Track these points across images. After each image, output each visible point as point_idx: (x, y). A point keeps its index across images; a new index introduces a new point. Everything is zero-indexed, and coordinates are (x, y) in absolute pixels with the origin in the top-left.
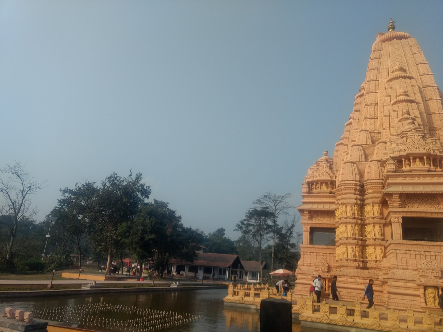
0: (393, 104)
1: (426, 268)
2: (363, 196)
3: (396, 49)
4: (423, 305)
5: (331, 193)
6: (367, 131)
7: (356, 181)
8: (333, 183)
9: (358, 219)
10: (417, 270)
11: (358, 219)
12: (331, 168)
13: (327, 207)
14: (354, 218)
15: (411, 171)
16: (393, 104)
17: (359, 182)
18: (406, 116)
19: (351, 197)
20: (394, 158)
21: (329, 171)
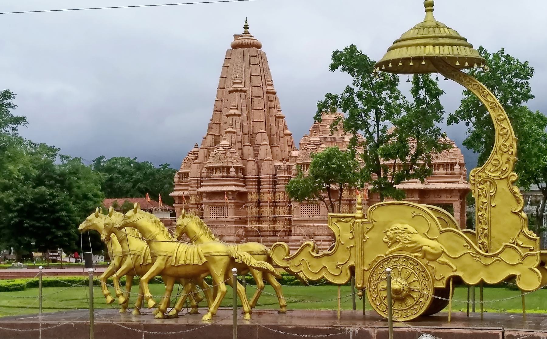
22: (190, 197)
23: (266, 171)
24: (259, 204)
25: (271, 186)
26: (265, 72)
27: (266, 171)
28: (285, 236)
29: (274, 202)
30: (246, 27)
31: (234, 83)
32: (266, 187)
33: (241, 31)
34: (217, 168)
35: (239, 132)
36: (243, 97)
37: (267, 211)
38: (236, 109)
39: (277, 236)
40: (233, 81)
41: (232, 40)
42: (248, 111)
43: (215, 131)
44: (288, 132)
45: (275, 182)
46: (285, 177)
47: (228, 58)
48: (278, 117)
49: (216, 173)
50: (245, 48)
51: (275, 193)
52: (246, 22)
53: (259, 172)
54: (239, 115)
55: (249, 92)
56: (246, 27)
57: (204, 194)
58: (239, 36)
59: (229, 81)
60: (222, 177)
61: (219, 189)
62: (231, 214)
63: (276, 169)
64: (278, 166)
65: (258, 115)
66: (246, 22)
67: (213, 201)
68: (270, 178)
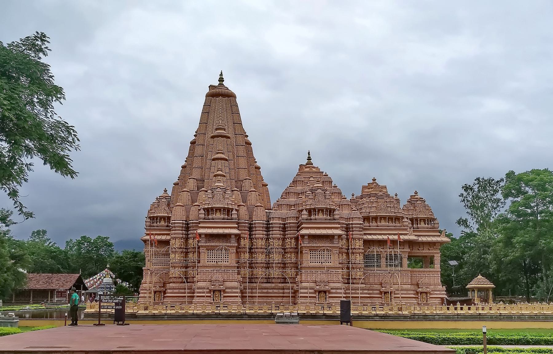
0: (214, 160)
2: (188, 231)
4: (212, 301)
5: (167, 226)
8: (169, 218)
9: (183, 248)
11: (183, 248)
12: (168, 205)
13: (164, 238)
14: (181, 248)
15: (213, 219)
16: (214, 160)
17: (186, 221)
19: (179, 233)
20: (204, 209)
21: (167, 209)
23: (259, 217)
25: (265, 233)
26: (238, 123)
27: (259, 217)
28: (280, 283)
30: (221, 80)
31: (216, 129)
32: (259, 233)
33: (216, 83)
35: (228, 175)
37: (260, 258)
40: (215, 127)
41: (207, 90)
43: (196, 174)
45: (268, 228)
46: (280, 224)
47: (207, 106)
49: (216, 214)
50: (220, 97)
51: (267, 239)
52: (221, 75)
53: (251, 218)
54: (226, 160)
59: (210, 128)
60: (223, 219)
61: (221, 231)
62: (232, 260)
63: (268, 216)
65: (243, 163)
66: (221, 75)
68: (263, 224)
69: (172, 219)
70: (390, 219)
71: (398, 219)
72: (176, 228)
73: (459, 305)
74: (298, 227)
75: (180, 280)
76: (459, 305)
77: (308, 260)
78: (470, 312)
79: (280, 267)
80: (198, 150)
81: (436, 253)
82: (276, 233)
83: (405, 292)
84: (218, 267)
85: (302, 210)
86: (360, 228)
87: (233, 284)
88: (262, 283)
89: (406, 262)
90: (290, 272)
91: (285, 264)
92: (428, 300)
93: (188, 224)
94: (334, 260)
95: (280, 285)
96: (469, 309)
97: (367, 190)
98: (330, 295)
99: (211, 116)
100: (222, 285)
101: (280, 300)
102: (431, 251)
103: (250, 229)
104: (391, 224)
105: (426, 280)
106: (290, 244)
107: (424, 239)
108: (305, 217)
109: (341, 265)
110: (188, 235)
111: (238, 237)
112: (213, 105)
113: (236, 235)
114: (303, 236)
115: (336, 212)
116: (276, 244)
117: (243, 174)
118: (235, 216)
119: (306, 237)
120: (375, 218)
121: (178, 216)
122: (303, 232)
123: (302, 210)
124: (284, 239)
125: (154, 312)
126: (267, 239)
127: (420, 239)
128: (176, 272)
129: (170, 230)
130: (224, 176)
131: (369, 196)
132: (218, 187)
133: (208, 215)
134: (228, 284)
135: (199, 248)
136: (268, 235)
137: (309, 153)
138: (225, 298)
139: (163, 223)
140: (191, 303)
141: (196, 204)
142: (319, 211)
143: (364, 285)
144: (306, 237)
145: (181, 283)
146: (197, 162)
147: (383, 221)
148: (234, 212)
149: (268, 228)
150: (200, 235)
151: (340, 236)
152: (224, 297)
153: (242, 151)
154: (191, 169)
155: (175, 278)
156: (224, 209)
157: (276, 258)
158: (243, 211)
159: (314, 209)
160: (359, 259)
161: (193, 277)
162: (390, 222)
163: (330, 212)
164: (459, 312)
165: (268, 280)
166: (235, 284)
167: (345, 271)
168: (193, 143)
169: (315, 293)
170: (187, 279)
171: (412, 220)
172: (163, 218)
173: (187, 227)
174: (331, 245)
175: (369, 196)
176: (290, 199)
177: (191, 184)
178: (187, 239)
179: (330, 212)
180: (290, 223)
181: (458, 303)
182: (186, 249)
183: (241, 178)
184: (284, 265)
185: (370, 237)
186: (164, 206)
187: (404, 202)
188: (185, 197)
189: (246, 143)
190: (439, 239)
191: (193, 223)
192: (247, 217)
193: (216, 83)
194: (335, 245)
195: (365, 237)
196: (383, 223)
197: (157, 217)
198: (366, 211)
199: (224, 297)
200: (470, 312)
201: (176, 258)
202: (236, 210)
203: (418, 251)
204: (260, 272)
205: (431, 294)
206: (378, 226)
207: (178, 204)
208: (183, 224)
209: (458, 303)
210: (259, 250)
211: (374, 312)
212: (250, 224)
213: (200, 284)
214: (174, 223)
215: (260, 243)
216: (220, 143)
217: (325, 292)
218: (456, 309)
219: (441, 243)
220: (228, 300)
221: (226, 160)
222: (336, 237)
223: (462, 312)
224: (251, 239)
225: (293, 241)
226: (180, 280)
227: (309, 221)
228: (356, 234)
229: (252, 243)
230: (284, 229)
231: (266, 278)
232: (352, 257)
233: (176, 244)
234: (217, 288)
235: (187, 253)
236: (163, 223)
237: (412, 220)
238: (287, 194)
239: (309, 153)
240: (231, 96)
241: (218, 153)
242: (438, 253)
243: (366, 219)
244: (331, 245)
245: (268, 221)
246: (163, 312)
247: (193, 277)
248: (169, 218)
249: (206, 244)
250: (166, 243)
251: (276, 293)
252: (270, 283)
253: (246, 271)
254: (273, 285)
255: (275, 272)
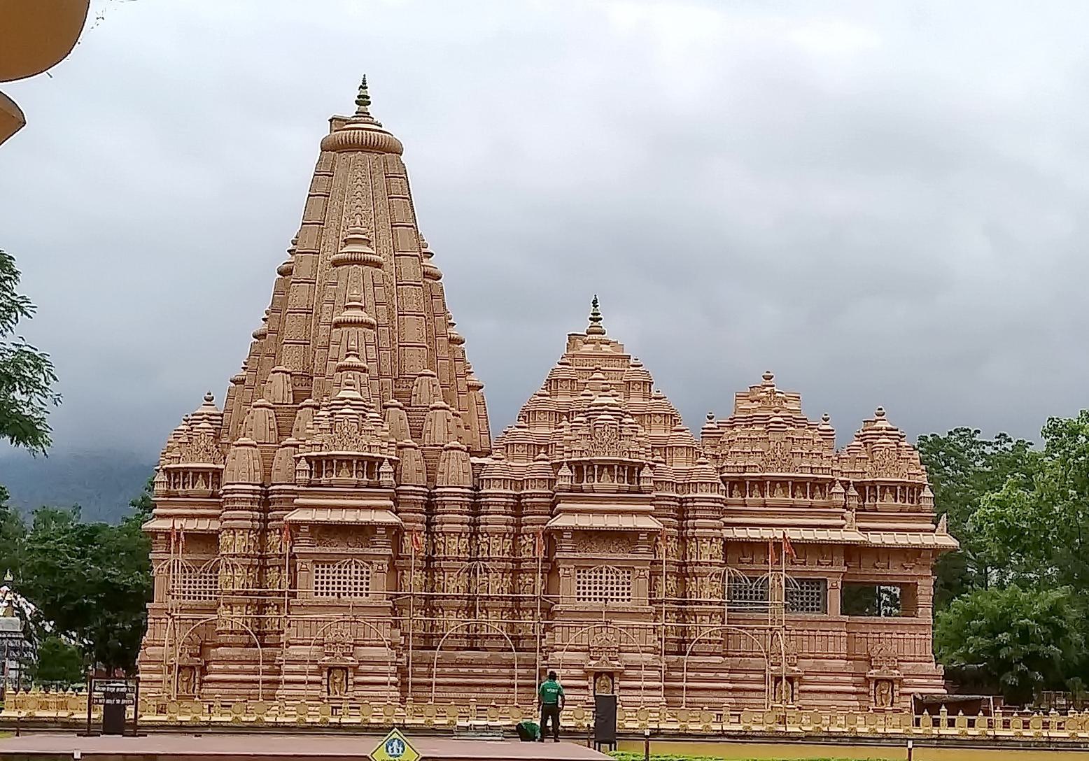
0: (337, 325)
1: (334, 641)
3: (359, 181)
4: (325, 695)
6: (286, 373)
7: (253, 485)
8: (218, 473)
10: (322, 645)
11: (254, 556)
12: (217, 437)
13: (203, 525)
16: (337, 325)
17: (262, 485)
18: (353, 360)
19: (243, 517)
22: (225, 538)
23: (454, 475)
24: (430, 565)
27: (454, 475)
29: (429, 560)
30: (363, 101)
32: (453, 520)
33: (350, 110)
34: (347, 461)
35: (373, 367)
36: (378, 281)
37: (453, 584)
38: (362, 308)
39: (435, 648)
42: (390, 313)
43: (291, 360)
44: (474, 379)
45: (476, 506)
47: (323, 173)
48: (452, 341)
50: (359, 148)
51: (474, 535)
52: (363, 87)
54: (371, 326)
55: (389, 268)
56: (363, 101)
57: (305, 529)
58: (347, 121)
59: (330, 237)
61: (350, 517)
62: (377, 591)
63: (476, 475)
64: (483, 465)
65: (414, 331)
66: (363, 87)
67: (328, 550)
69: (227, 477)
70: (798, 485)
71: (819, 485)
72: (236, 505)
73: (944, 716)
74: (553, 505)
75: (245, 639)
76: (944, 716)
77: (569, 591)
78: (971, 732)
79: (504, 609)
80: (300, 296)
81: (921, 577)
82: (496, 520)
83: (831, 678)
84: (341, 607)
85: (560, 465)
86: (714, 509)
87: (378, 649)
88: (458, 649)
89: (834, 599)
90: (529, 622)
91: (517, 600)
92: (896, 700)
93: (267, 494)
94: (636, 594)
95: (505, 655)
96: (971, 724)
97: (747, 405)
98: (622, 683)
99: (334, 204)
100: (351, 655)
101: (501, 694)
102: (907, 572)
103: (430, 507)
104: (799, 499)
105: (893, 649)
106: (533, 550)
107: (889, 540)
108: (564, 483)
109: (653, 608)
110: (266, 521)
111: (395, 533)
112: (339, 172)
113: (389, 527)
114: (560, 531)
115: (646, 472)
116: (497, 547)
117: (415, 362)
118: (387, 479)
119: (567, 536)
120: (760, 484)
121: (241, 471)
122: (562, 521)
123: (560, 465)
124: (517, 536)
125: (180, 718)
126: (474, 535)
127: (875, 539)
128: (233, 618)
129: (220, 506)
130: (365, 370)
131: (750, 421)
132: (345, 402)
133: (319, 474)
134: (366, 652)
135: (293, 557)
136: (475, 524)
137: (595, 303)
138: (357, 688)
139: (201, 487)
140: (272, 697)
141: (290, 440)
142: (601, 467)
143: (719, 659)
144: (567, 536)
145: (247, 646)
146: (294, 327)
147: (779, 491)
148: (386, 467)
149: (476, 506)
150: (296, 526)
151: (652, 533)
152: (356, 684)
153: (414, 300)
154: (278, 344)
155: (232, 632)
156: (360, 459)
157: (496, 585)
158: (412, 462)
159: (590, 464)
160: (707, 590)
161: (279, 633)
162: (799, 494)
163: (631, 470)
164: (945, 731)
165: (473, 641)
166: (384, 653)
167: (672, 623)
168: (285, 272)
169: (585, 678)
170: (262, 636)
171: (860, 487)
172: (204, 473)
173: (265, 501)
174: (629, 556)
175: (750, 421)
176: (539, 430)
177: (279, 387)
178: (264, 532)
179: (631, 470)
180: (532, 496)
181: (943, 709)
182: (260, 557)
183: (409, 371)
184: (516, 605)
185: (740, 534)
186: (204, 441)
187: (847, 436)
188: (260, 421)
189: (426, 274)
190: (928, 540)
191: (279, 492)
192: (422, 479)
193: (350, 110)
194: (640, 557)
195: (728, 533)
196: (779, 497)
197: (186, 471)
198: (734, 464)
199: (356, 684)
200: (971, 732)
201: (235, 579)
202: (390, 460)
203: (874, 571)
204: (452, 622)
205: (902, 685)
206: (765, 506)
207: (242, 440)
208: (254, 492)
209: (943, 709)
210: (451, 564)
211: (718, 727)
212: (430, 495)
213: (295, 651)
214: (232, 491)
215: (455, 546)
216: (355, 283)
217: (611, 675)
218: (936, 723)
219: (935, 550)
220: (361, 691)
221: (371, 326)
222: (643, 537)
223: (952, 731)
224: (430, 533)
225: (540, 541)
226: (245, 639)
227: (575, 492)
228: (702, 525)
229: (434, 545)
230: (517, 508)
231: (468, 637)
232: (693, 585)
233: (235, 544)
234: (338, 662)
235: (263, 568)
236: (201, 487)
237: (858, 486)
238: (529, 415)
239: (595, 303)
240: (389, 149)
241: (347, 307)
242: (928, 577)
243: (736, 484)
244: (629, 556)
245: (478, 489)
246: (203, 719)
247: (279, 633)
248: (218, 473)
249: (312, 550)
250: (209, 540)
251: (478, 676)
252: (478, 649)
253: (414, 619)
254: (486, 655)
255: (493, 623)
